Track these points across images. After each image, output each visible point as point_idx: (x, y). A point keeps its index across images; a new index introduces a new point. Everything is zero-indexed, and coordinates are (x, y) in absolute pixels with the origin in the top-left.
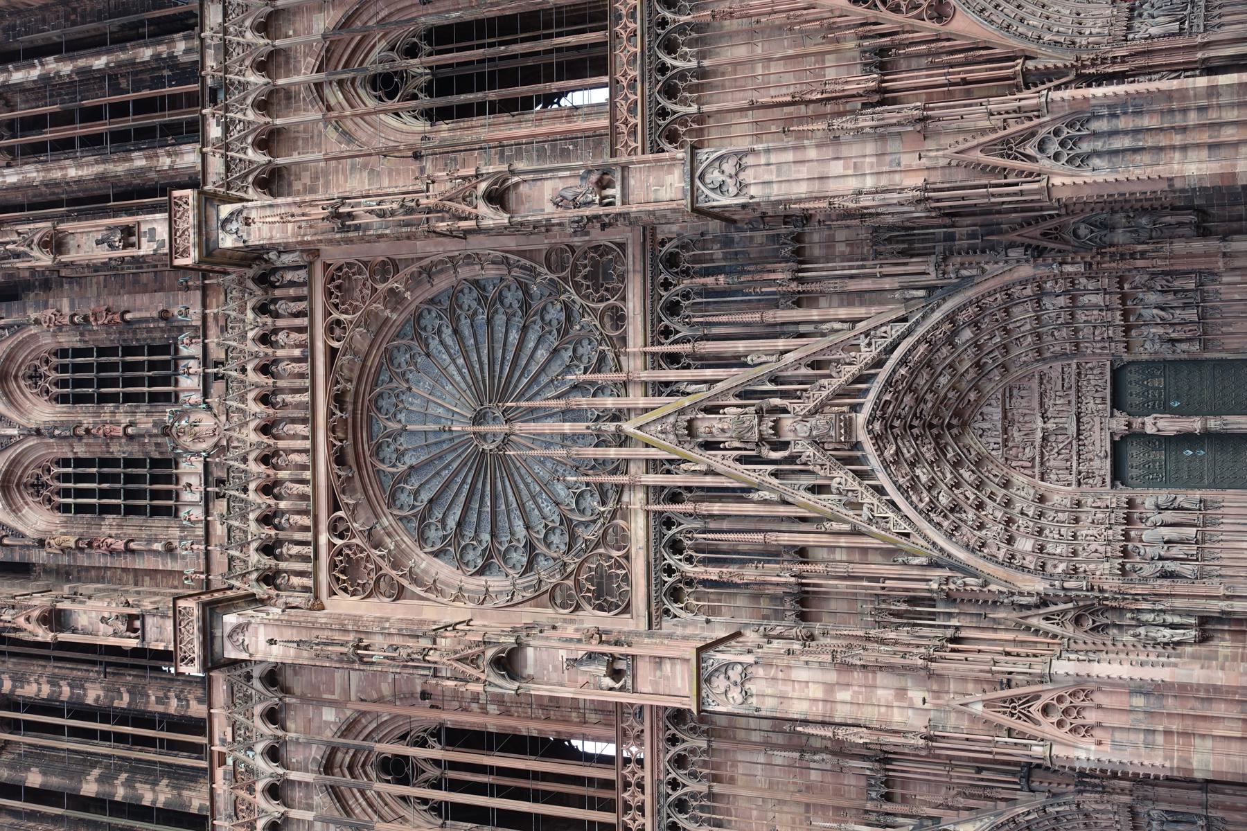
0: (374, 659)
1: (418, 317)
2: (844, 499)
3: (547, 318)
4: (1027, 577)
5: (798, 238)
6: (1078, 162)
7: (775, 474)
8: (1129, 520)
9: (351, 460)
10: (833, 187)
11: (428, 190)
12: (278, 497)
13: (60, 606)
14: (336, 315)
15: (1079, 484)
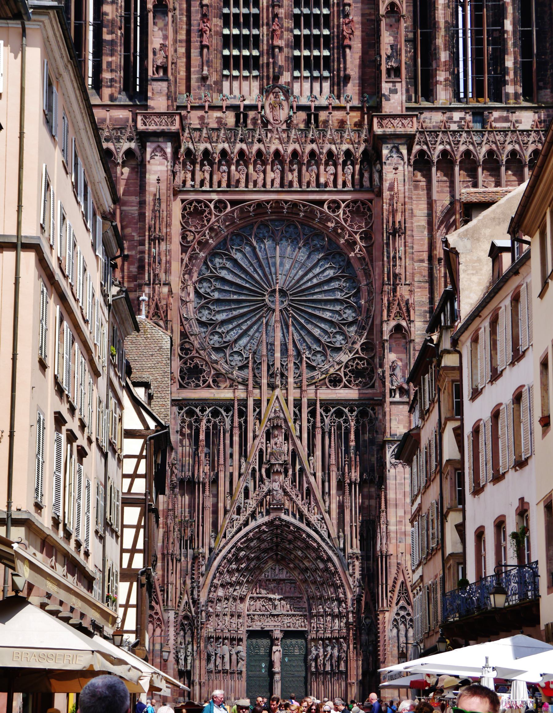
0: (153, 250)
1: (341, 254)
2: (242, 506)
3: (338, 336)
4: (206, 594)
5: (372, 481)
6: (395, 623)
7: (254, 470)
8: (232, 639)
9: (260, 211)
10: (391, 511)
11: (405, 285)
12: (238, 164)
13: (170, 14)
14: (343, 205)
15: (248, 615)
